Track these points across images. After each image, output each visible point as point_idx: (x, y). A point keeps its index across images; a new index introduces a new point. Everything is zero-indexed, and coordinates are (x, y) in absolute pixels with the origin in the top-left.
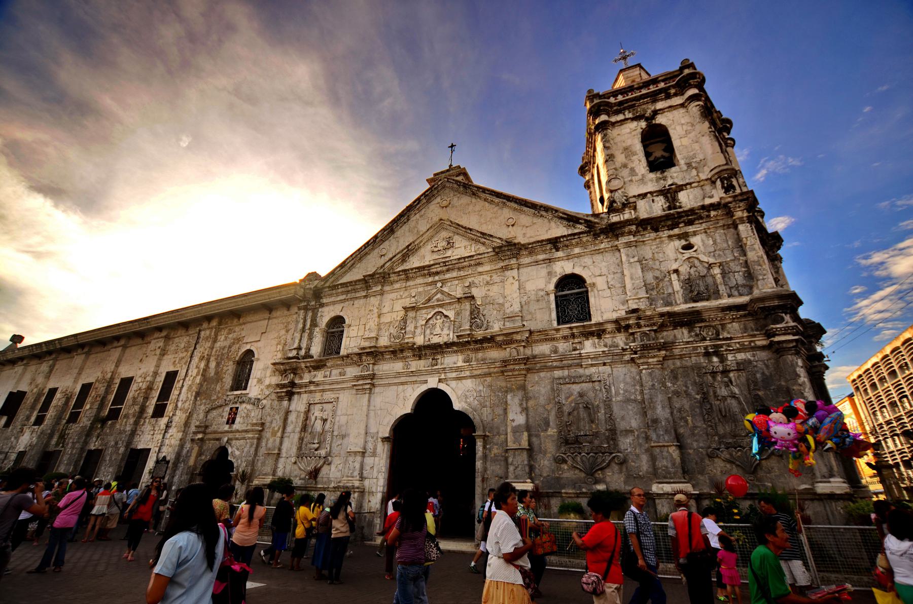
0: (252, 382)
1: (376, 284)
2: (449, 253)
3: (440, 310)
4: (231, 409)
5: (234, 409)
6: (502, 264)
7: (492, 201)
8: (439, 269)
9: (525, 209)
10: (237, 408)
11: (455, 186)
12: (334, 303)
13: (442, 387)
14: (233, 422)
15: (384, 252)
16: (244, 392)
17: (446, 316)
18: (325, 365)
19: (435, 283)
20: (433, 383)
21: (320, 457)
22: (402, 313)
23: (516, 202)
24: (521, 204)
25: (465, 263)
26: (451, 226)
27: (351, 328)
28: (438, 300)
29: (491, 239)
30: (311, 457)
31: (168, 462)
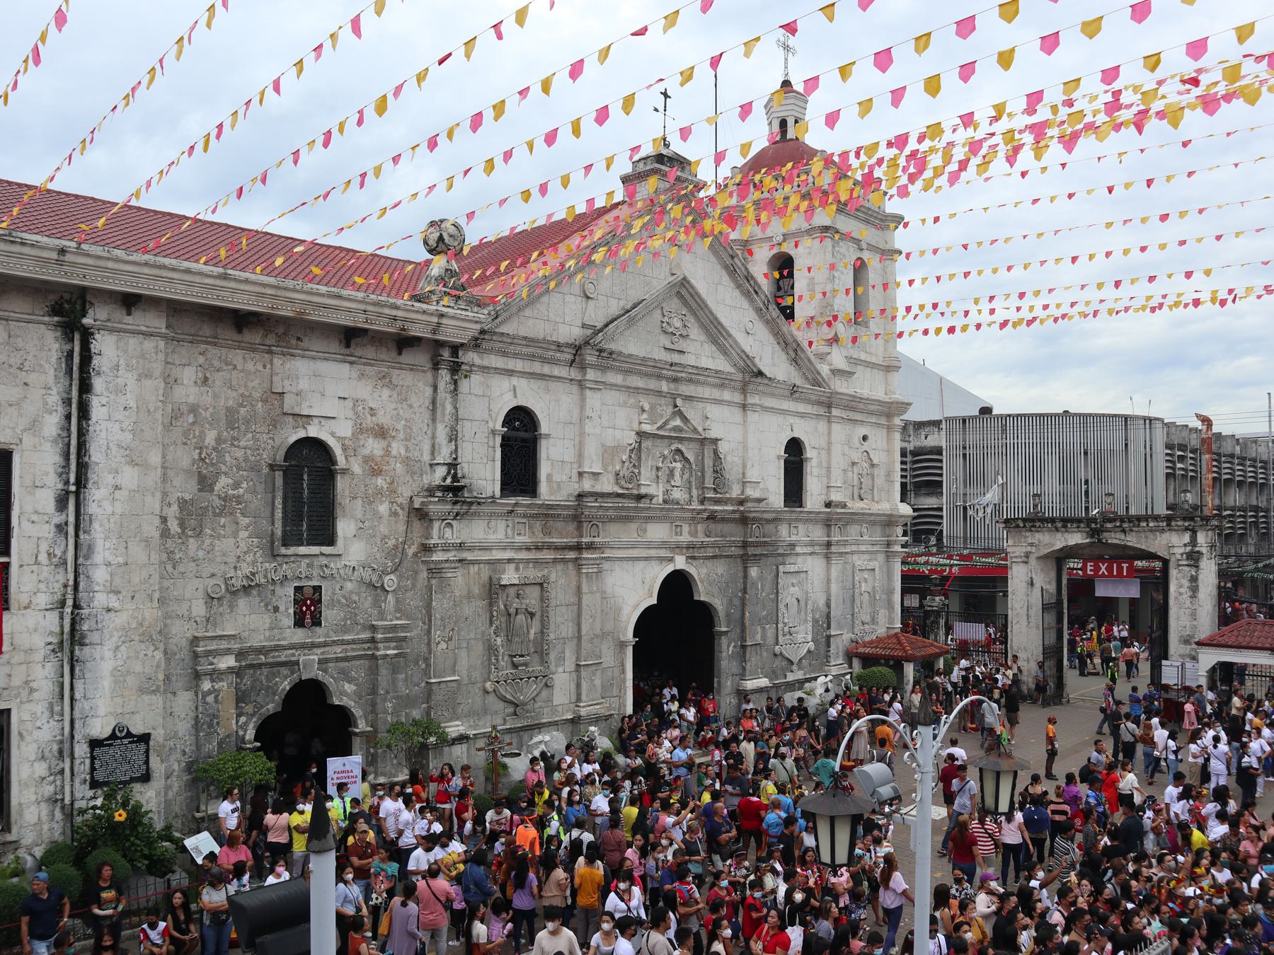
0: (344, 527)
1: (593, 366)
2: (682, 345)
3: (680, 446)
4: (298, 589)
10: (317, 589)
12: (510, 373)
13: (692, 570)
14: (316, 622)
15: (590, 289)
16: (326, 550)
17: (686, 460)
19: (674, 397)
20: (680, 563)
21: (536, 678)
22: (631, 438)
27: (551, 441)
28: (676, 429)
30: (521, 679)
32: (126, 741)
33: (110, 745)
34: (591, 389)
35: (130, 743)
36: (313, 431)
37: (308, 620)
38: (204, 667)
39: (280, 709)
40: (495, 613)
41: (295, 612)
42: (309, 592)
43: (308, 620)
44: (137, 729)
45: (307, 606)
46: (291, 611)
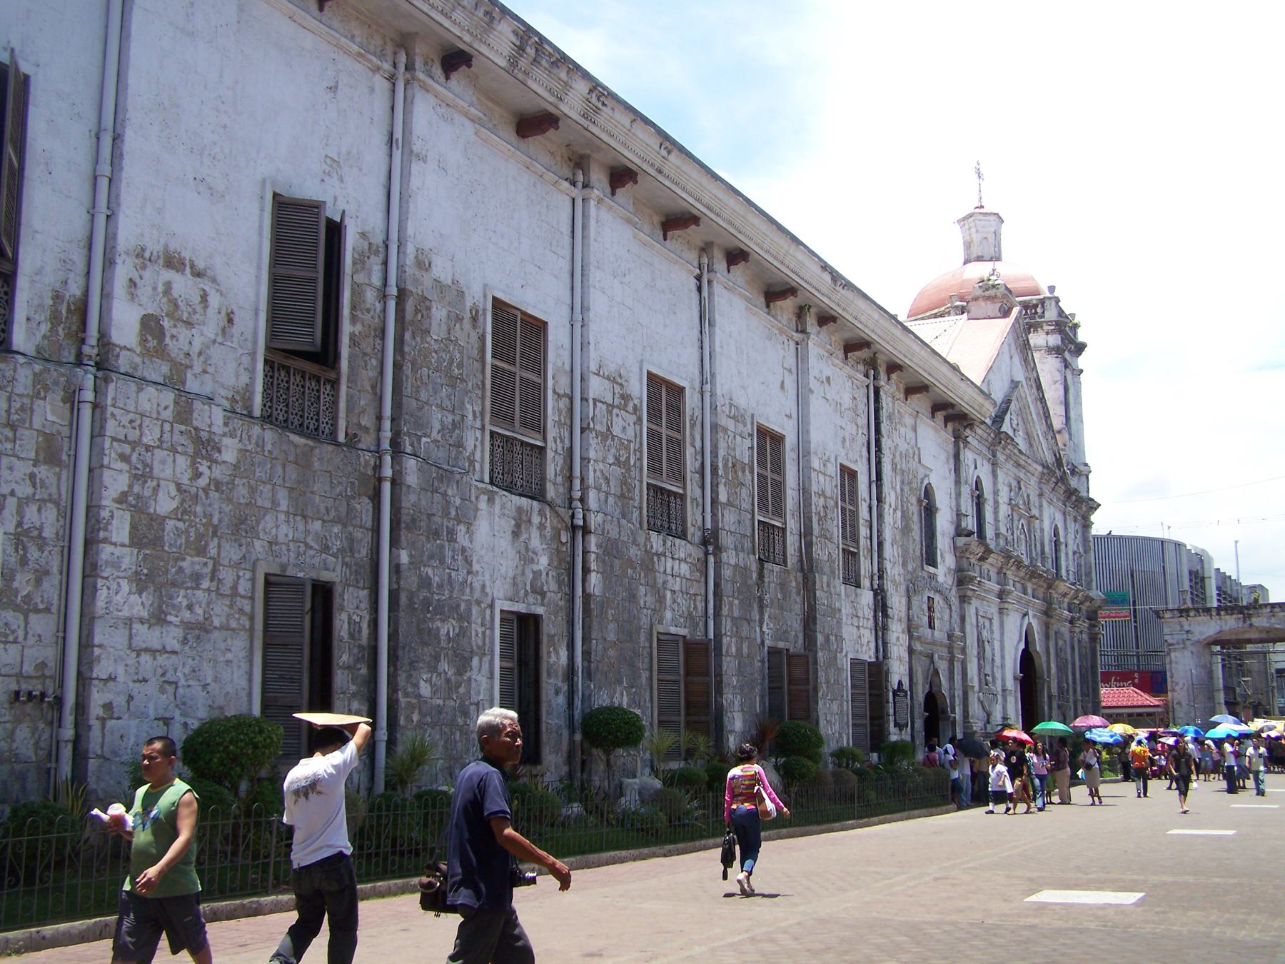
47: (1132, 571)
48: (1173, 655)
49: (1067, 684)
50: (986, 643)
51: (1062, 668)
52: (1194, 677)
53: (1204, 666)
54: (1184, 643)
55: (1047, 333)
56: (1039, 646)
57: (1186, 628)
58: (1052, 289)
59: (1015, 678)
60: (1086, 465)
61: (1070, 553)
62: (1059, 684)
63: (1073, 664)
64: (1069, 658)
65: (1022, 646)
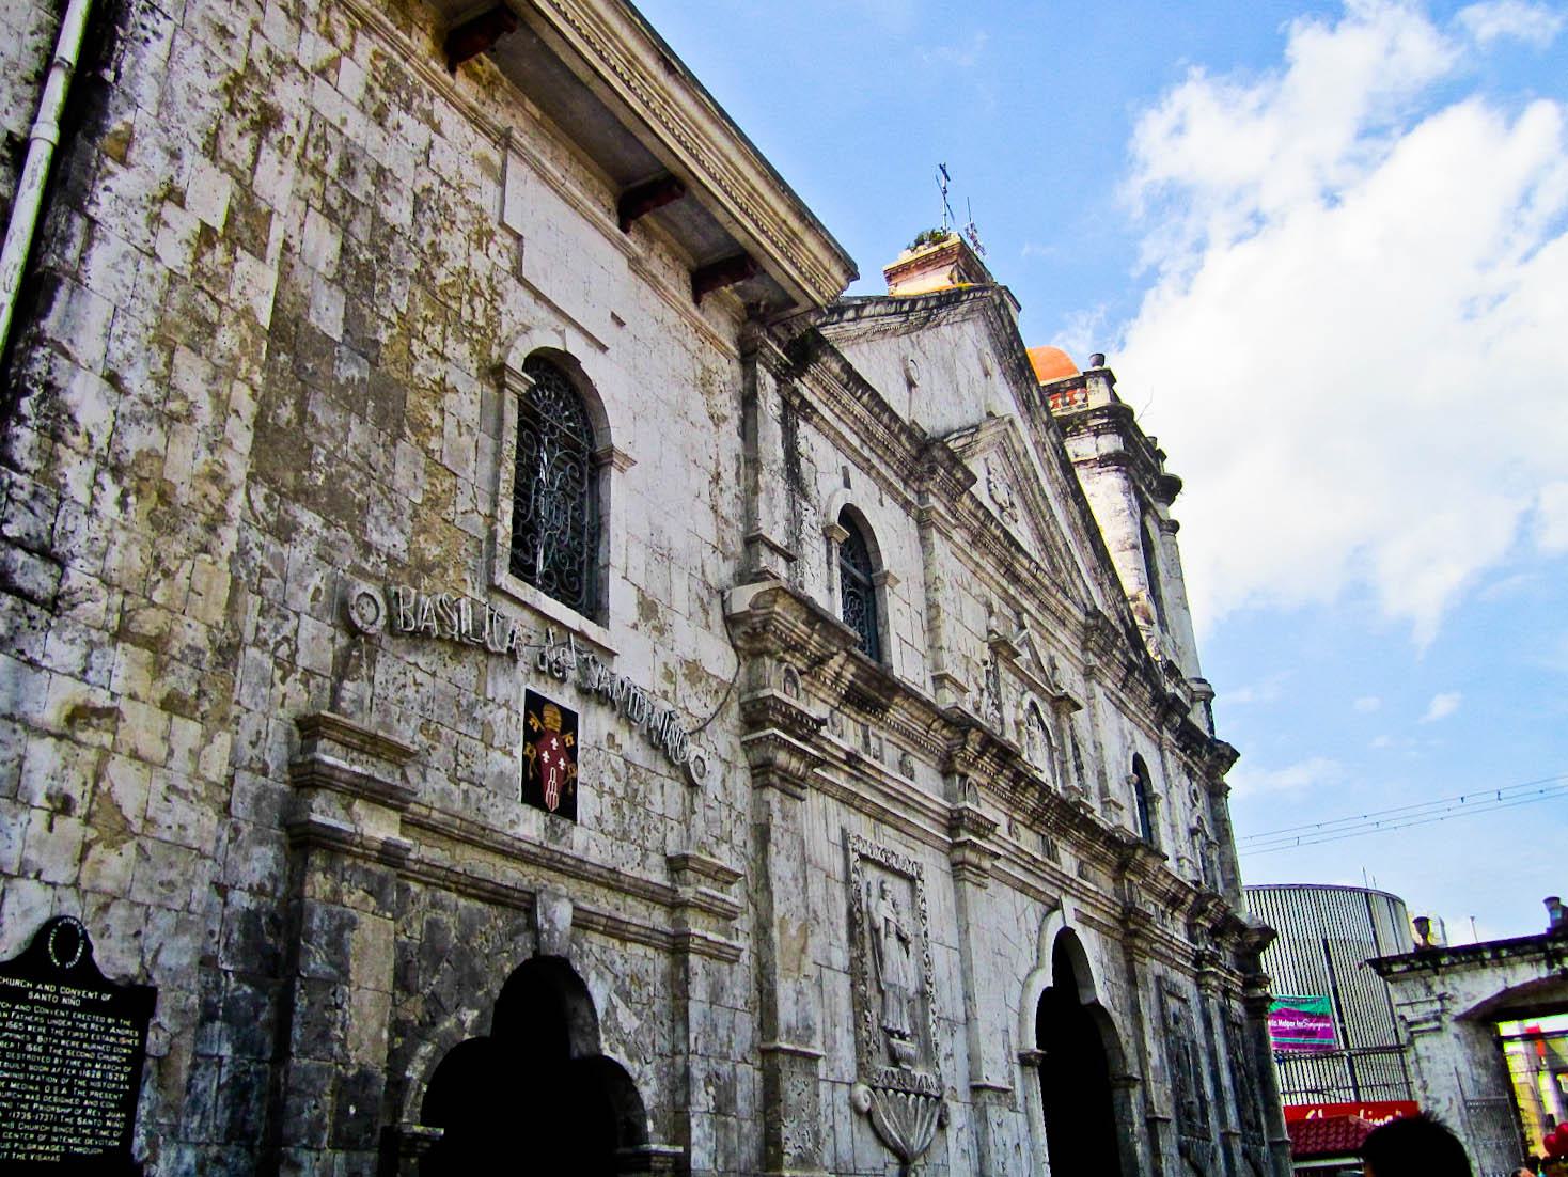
4: (535, 703)
5: (552, 720)
6: (1078, 653)
7: (1049, 463)
8: (1025, 574)
9: (1088, 544)
10: (569, 721)
11: (1003, 336)
14: (568, 809)
16: (592, 630)
18: (885, 710)
23: (1083, 517)
24: (1087, 529)
25: (1053, 601)
26: (1018, 458)
29: (1074, 574)
31: (135, 1001)
32: (72, 996)
33: (18, 996)
34: (939, 531)
35: (87, 1006)
36: (576, 346)
37: (552, 794)
38: (324, 812)
39: (487, 1031)
40: (858, 916)
41: (525, 758)
42: (552, 720)
43: (552, 794)
44: (113, 957)
45: (551, 752)
46: (518, 751)
47: (1325, 941)
48: (1420, 1043)
49: (1202, 1098)
50: (891, 945)
51: (1180, 1058)
52: (1468, 1085)
53: (1484, 1064)
54: (1438, 1019)
55: (1097, 434)
56: (1103, 989)
57: (1438, 989)
58: (1100, 359)
59: (1025, 1061)
60: (1201, 681)
61: (1183, 833)
62: (1179, 1090)
63: (1213, 1055)
64: (1201, 1042)
65: (1045, 979)
